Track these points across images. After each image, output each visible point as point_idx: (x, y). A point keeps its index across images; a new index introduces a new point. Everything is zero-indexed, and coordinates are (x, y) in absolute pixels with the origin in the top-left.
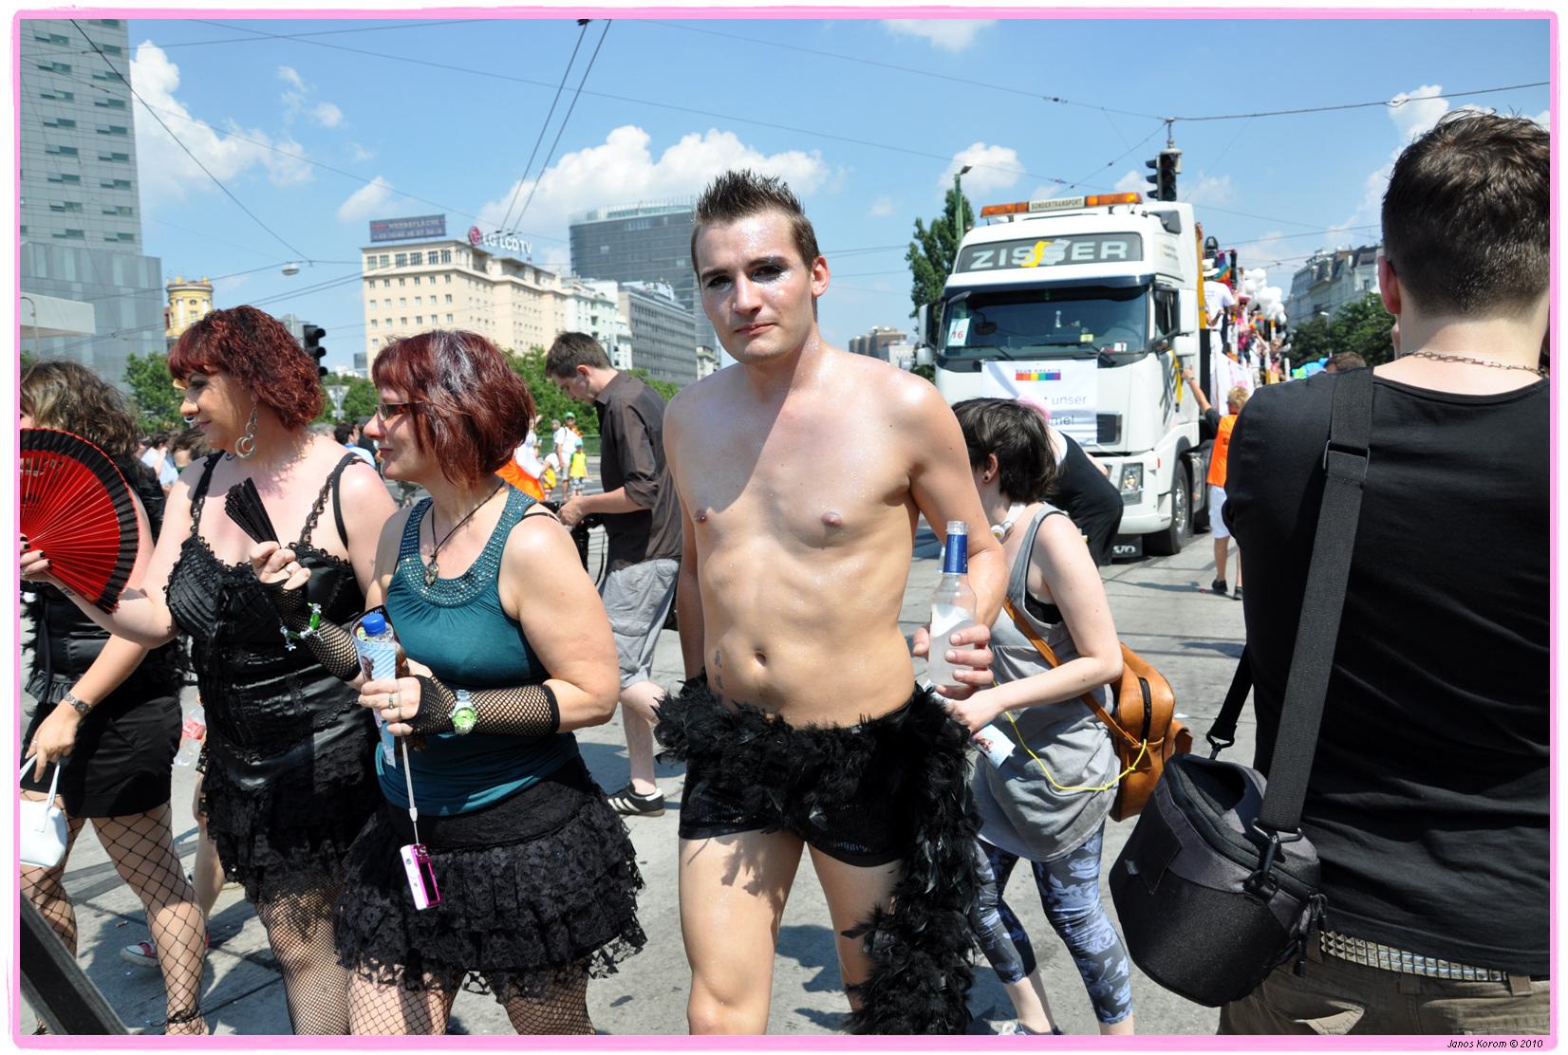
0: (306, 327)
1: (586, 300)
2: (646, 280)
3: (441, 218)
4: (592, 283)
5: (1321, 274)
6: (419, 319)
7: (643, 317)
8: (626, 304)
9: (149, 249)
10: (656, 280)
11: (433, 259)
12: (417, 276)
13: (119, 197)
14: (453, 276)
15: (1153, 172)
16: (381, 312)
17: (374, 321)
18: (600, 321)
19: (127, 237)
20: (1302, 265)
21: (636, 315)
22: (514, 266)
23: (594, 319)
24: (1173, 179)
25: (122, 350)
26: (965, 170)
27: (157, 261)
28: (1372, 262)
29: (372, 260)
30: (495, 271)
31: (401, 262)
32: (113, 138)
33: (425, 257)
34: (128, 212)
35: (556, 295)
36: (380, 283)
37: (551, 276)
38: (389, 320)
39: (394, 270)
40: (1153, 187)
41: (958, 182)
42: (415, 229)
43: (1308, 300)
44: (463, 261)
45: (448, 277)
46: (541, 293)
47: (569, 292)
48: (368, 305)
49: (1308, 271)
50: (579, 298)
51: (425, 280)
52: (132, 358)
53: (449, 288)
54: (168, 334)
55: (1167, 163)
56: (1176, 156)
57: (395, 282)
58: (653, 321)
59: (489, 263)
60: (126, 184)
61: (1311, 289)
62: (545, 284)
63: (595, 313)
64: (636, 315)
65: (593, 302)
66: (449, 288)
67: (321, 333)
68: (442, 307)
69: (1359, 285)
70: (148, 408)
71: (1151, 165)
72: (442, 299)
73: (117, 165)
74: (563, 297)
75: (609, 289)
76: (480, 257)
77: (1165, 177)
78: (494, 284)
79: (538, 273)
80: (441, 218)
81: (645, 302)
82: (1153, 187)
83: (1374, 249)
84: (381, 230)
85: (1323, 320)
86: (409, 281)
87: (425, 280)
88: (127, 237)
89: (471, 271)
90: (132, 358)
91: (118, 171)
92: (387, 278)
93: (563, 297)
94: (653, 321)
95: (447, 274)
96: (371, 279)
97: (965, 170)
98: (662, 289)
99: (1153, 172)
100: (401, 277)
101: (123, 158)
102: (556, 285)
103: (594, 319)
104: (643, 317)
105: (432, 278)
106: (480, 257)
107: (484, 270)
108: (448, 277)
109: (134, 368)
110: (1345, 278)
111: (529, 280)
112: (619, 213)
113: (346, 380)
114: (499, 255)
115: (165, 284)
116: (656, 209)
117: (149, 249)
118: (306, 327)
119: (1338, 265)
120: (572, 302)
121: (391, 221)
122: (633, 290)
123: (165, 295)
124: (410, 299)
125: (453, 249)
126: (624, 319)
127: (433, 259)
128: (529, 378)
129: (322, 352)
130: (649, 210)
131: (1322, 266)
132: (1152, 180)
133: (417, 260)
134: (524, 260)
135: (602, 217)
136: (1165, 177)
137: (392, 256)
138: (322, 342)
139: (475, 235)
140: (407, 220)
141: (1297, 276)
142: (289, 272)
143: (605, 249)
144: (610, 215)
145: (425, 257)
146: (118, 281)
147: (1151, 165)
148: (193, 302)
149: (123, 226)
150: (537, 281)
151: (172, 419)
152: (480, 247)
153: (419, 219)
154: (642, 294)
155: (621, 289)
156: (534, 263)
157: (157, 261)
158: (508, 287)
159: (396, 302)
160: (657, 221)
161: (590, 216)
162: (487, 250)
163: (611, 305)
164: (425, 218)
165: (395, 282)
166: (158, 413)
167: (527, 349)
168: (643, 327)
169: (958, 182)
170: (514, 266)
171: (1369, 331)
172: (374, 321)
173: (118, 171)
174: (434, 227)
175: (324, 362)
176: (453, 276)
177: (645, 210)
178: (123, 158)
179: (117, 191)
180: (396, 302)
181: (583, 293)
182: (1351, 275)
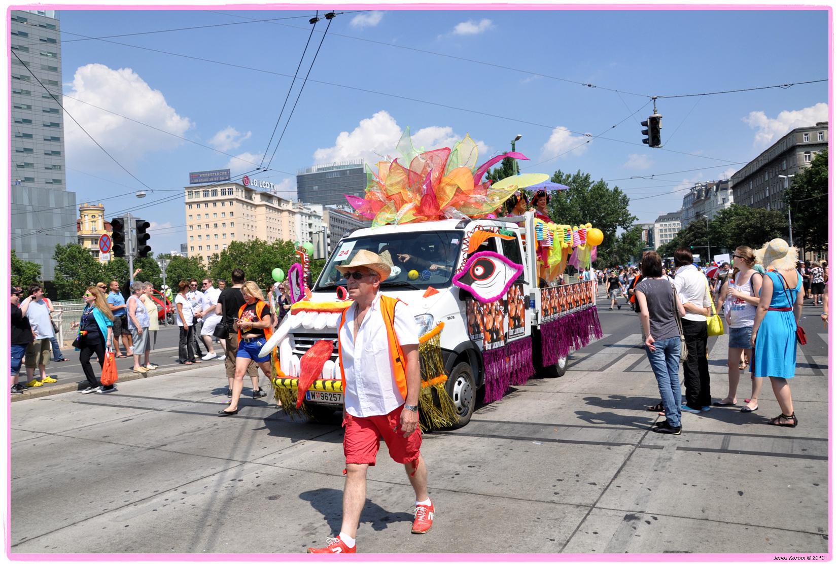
0: (138, 221)
1: (306, 214)
2: (338, 204)
3: (229, 170)
4: (309, 205)
5: (699, 196)
6: (216, 225)
7: (337, 224)
8: (327, 217)
9: (69, 188)
10: (343, 203)
11: (223, 193)
12: (215, 202)
13: (54, 160)
14: (234, 202)
15: (646, 128)
16: (195, 221)
17: (191, 226)
18: (313, 226)
19: (58, 181)
20: (689, 191)
21: (333, 223)
22: (267, 196)
23: (310, 225)
24: (658, 132)
25: (53, 244)
26: (518, 138)
27: (74, 194)
28: (726, 189)
29: (190, 193)
30: (257, 199)
31: (206, 195)
32: (52, 129)
33: (219, 193)
34: (59, 168)
35: (289, 211)
36: (194, 206)
37: (287, 202)
38: (199, 226)
39: (201, 198)
40: (646, 137)
41: (513, 145)
42: (214, 176)
43: (693, 209)
44: (240, 195)
45: (231, 203)
46: (282, 211)
47: (297, 210)
48: (188, 218)
49: (692, 194)
50: (302, 214)
51: (219, 204)
52: (58, 247)
53: (232, 209)
54: (79, 234)
55: (654, 121)
56: (659, 118)
57: (202, 205)
58: (342, 225)
59: (254, 195)
60: (58, 153)
61: (694, 204)
62: (284, 206)
63: (310, 222)
64: (333, 223)
65: (310, 216)
66: (232, 209)
67: (147, 225)
68: (228, 219)
69: (720, 202)
70: (67, 274)
71: (644, 124)
72: (228, 215)
73: (52, 143)
74: (294, 213)
75: (318, 209)
76: (249, 192)
77: (653, 133)
78: (257, 206)
79: (280, 200)
80: (229, 170)
81: (337, 215)
82: (646, 137)
83: (727, 182)
84: (195, 178)
85: (704, 219)
86: (210, 205)
87: (219, 204)
88: (58, 181)
89: (244, 199)
90: (58, 247)
91: (54, 146)
92: (198, 203)
93: (294, 213)
94: (342, 225)
95: (231, 201)
96: (190, 204)
97: (518, 138)
98: (347, 209)
99: (646, 128)
100: (206, 203)
101: (57, 139)
102: (290, 207)
103: (310, 225)
104: (337, 224)
105: (223, 204)
106: (249, 192)
107: (251, 198)
108: (231, 203)
109: (59, 251)
110: (712, 197)
111: (275, 204)
112: (323, 169)
113: (175, 258)
114: (259, 190)
115: (78, 207)
116: (343, 166)
117: (69, 188)
118: (138, 221)
119: (708, 191)
120: (298, 216)
121: (201, 173)
122: (331, 209)
123: (78, 213)
124: (211, 215)
125: (234, 188)
126: (326, 225)
127: (223, 193)
128: (275, 256)
129: (148, 237)
130: (340, 167)
131: (700, 191)
132: (645, 133)
133: (215, 193)
134: (272, 194)
135: (314, 170)
136: (653, 133)
137: (201, 193)
138: (148, 231)
139: (246, 179)
140: (210, 172)
141: (686, 197)
142: (140, 196)
143: (316, 188)
144: (318, 169)
145: (219, 193)
146: (52, 205)
147: (644, 124)
148: (93, 216)
149: (55, 175)
150: (279, 205)
151: (79, 279)
152: (249, 186)
153: (216, 172)
154: (335, 211)
155: (324, 209)
156: (278, 195)
157: (74, 194)
158: (264, 208)
159: (203, 216)
160: (343, 173)
161: (307, 171)
162: (253, 188)
163: (319, 217)
164: (219, 171)
165: (202, 205)
166: (72, 276)
167: (274, 241)
168: (336, 229)
169: (513, 145)
170: (267, 196)
171: (733, 224)
172: (191, 226)
173: (54, 146)
174: (224, 176)
175: (148, 243)
176: (234, 202)
177: (337, 167)
178: (57, 139)
179: (53, 157)
180: (203, 216)
181: (305, 211)
182: (716, 196)
